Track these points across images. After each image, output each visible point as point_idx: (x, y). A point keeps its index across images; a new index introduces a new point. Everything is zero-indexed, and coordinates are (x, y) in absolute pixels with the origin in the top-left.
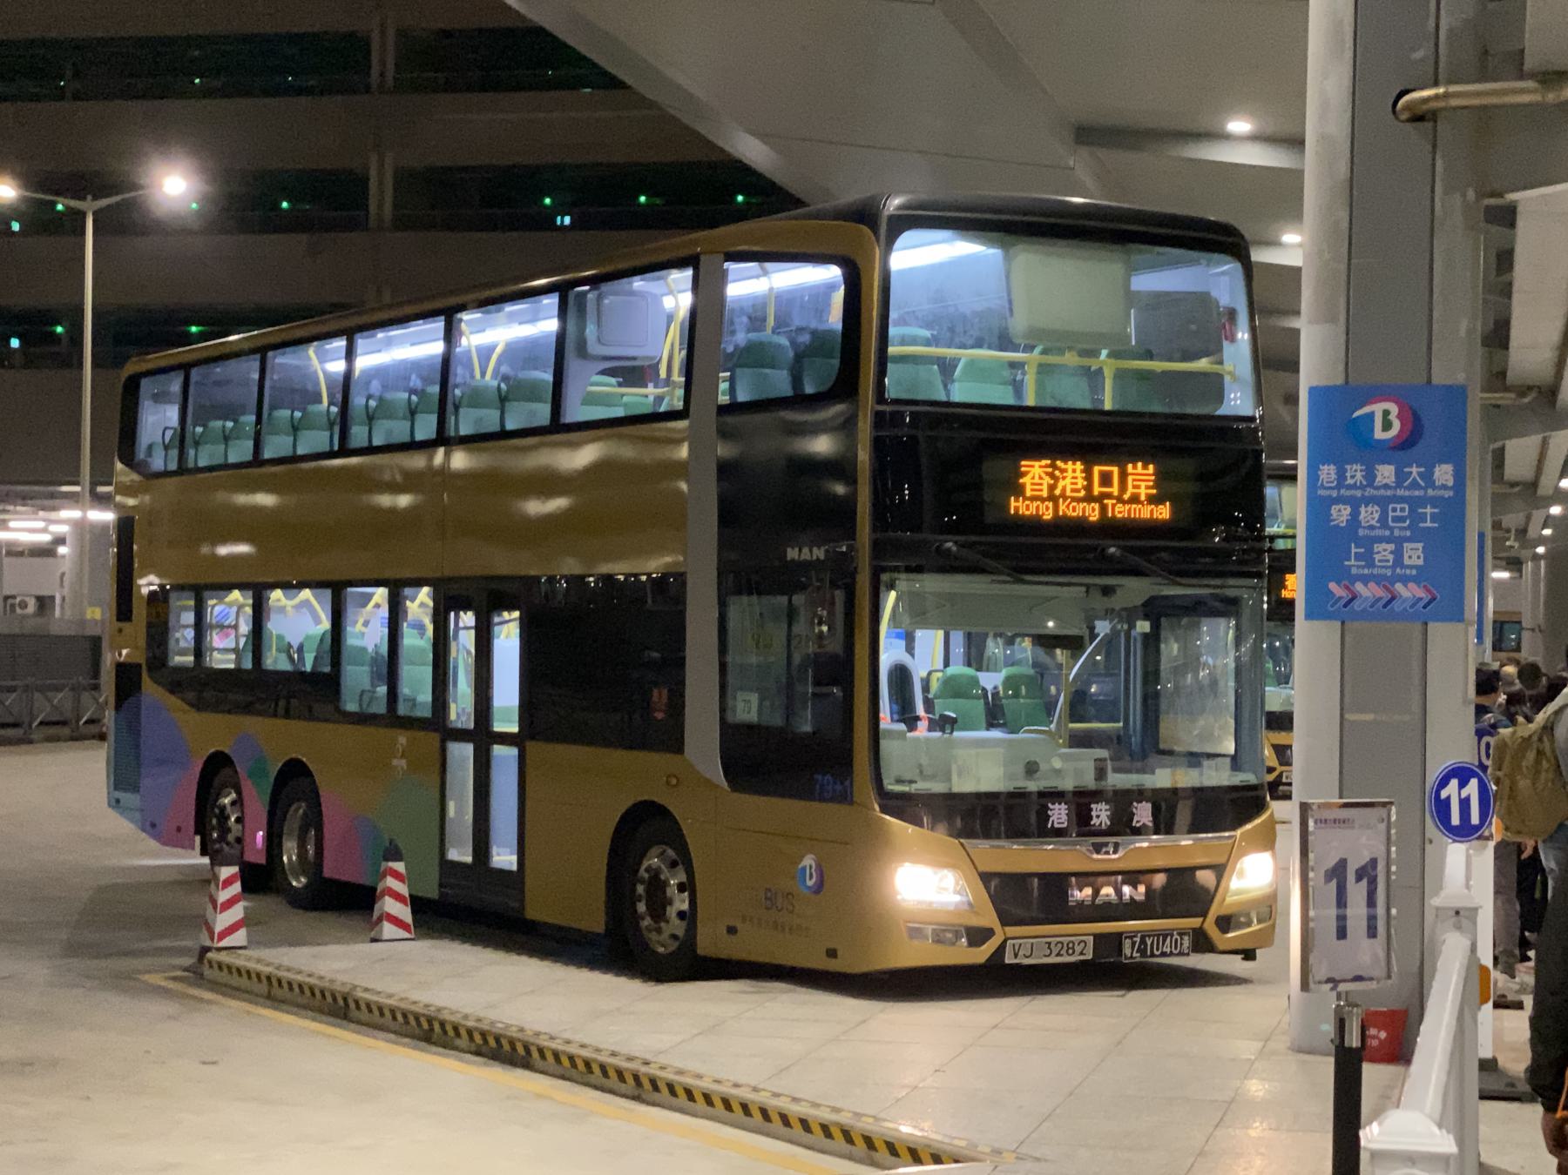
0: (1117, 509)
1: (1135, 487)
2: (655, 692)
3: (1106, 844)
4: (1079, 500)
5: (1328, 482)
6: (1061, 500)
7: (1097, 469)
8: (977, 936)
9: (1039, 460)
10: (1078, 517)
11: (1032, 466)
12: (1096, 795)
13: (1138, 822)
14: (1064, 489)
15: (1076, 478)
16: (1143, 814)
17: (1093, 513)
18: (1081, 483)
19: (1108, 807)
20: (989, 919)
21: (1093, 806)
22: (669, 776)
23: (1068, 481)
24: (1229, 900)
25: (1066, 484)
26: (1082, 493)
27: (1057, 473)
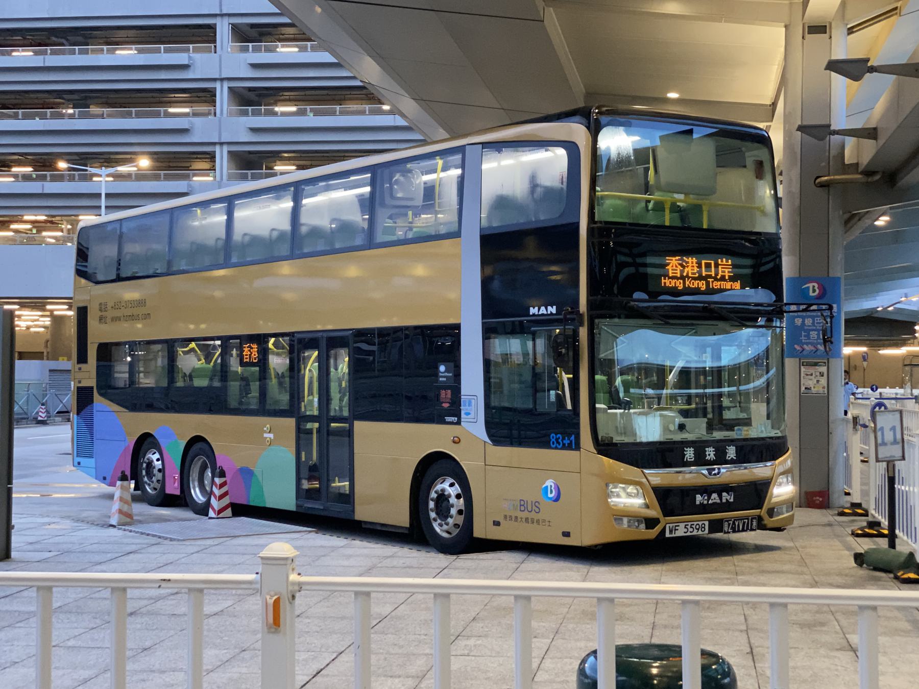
0: (714, 284)
1: (723, 272)
2: (443, 393)
3: (714, 469)
4: (695, 279)
7: (703, 262)
8: (651, 523)
9: (674, 256)
10: (695, 288)
11: (672, 260)
12: (707, 443)
13: (729, 457)
15: (693, 266)
16: (731, 452)
17: (702, 285)
18: (696, 269)
21: (707, 449)
22: (454, 438)
23: (690, 268)
24: (774, 500)
26: (697, 275)
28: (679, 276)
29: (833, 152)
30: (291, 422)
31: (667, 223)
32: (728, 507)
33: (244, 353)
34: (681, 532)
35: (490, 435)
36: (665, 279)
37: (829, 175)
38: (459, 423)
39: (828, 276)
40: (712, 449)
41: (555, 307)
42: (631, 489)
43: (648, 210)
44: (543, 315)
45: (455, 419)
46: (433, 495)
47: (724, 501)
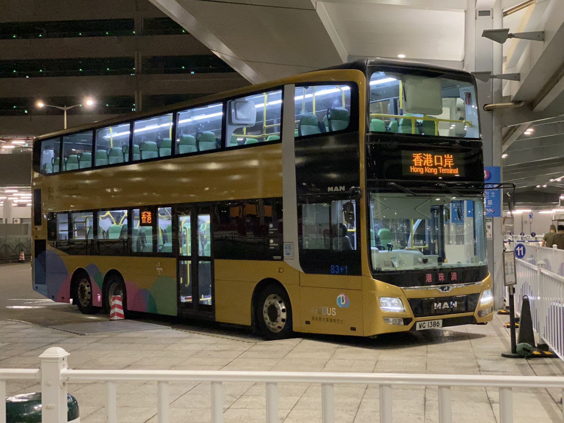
0: (442, 170)
3: (445, 287)
7: (435, 156)
8: (407, 321)
9: (418, 153)
10: (431, 173)
11: (416, 155)
14: (426, 163)
17: (435, 171)
18: (431, 161)
20: (409, 314)
21: (439, 274)
23: (427, 160)
28: (421, 165)
29: (495, 90)
30: (174, 260)
31: (413, 133)
33: (142, 218)
36: (412, 167)
37: (492, 103)
38: (282, 259)
39: (492, 165)
40: (442, 274)
41: (344, 187)
42: (395, 300)
43: (399, 125)
44: (336, 191)
45: (279, 257)
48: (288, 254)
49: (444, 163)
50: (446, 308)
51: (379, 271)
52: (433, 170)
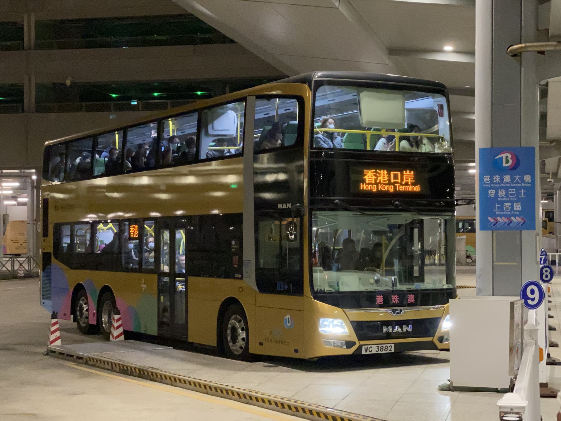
0: (400, 188)
3: (397, 310)
4: (386, 184)
5: (487, 182)
6: (379, 184)
7: (392, 173)
8: (349, 344)
9: (370, 169)
11: (368, 172)
12: (394, 292)
14: (380, 180)
18: (386, 178)
19: (398, 296)
23: (381, 177)
25: (381, 178)
26: (387, 182)
27: (377, 174)
28: (373, 182)
32: (406, 335)
34: (374, 350)
35: (258, 285)
36: (363, 185)
38: (241, 278)
40: (396, 296)
46: (230, 326)
47: (405, 330)
48: (247, 273)
49: (402, 180)
50: (398, 332)
51: (323, 292)
52: (388, 188)
